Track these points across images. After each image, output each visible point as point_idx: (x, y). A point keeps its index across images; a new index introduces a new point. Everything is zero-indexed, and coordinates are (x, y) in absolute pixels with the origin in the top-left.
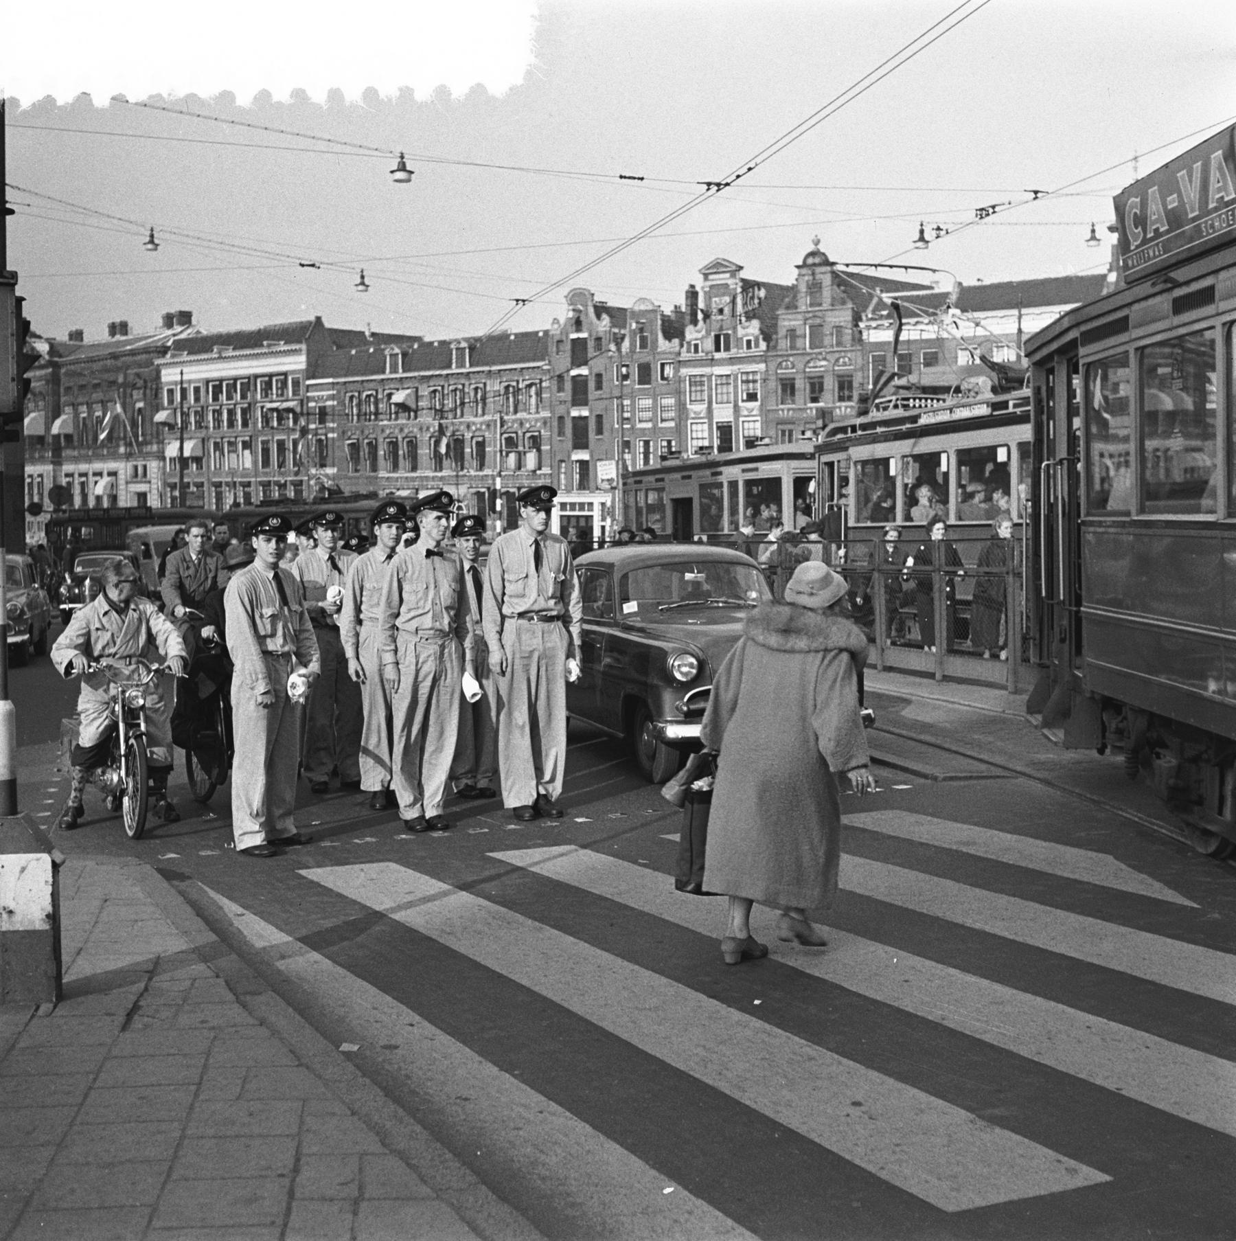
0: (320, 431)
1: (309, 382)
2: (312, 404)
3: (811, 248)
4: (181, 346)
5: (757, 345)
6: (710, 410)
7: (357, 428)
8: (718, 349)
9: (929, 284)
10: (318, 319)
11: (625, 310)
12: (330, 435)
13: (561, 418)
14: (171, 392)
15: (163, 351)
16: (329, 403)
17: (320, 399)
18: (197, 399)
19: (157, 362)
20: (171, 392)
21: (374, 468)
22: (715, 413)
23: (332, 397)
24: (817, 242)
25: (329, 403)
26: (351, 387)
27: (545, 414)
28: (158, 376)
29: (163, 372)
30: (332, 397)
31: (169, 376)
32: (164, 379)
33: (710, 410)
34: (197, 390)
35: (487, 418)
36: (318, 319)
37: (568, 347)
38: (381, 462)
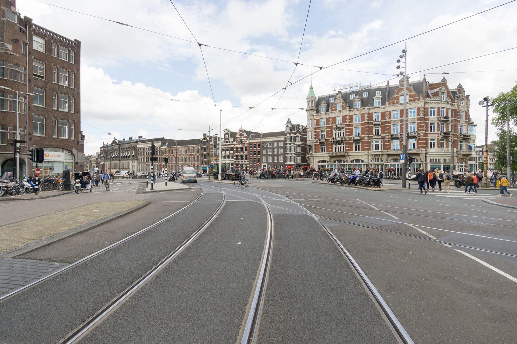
3: (240, 127)
4: (140, 141)
5: (232, 142)
6: (225, 153)
8: (226, 143)
9: (260, 133)
10: (163, 137)
11: (212, 136)
13: (202, 154)
14: (139, 149)
15: (137, 142)
20: (139, 149)
22: (226, 153)
24: (241, 126)
27: (200, 153)
33: (225, 153)
35: (190, 153)
36: (163, 137)
37: (203, 142)
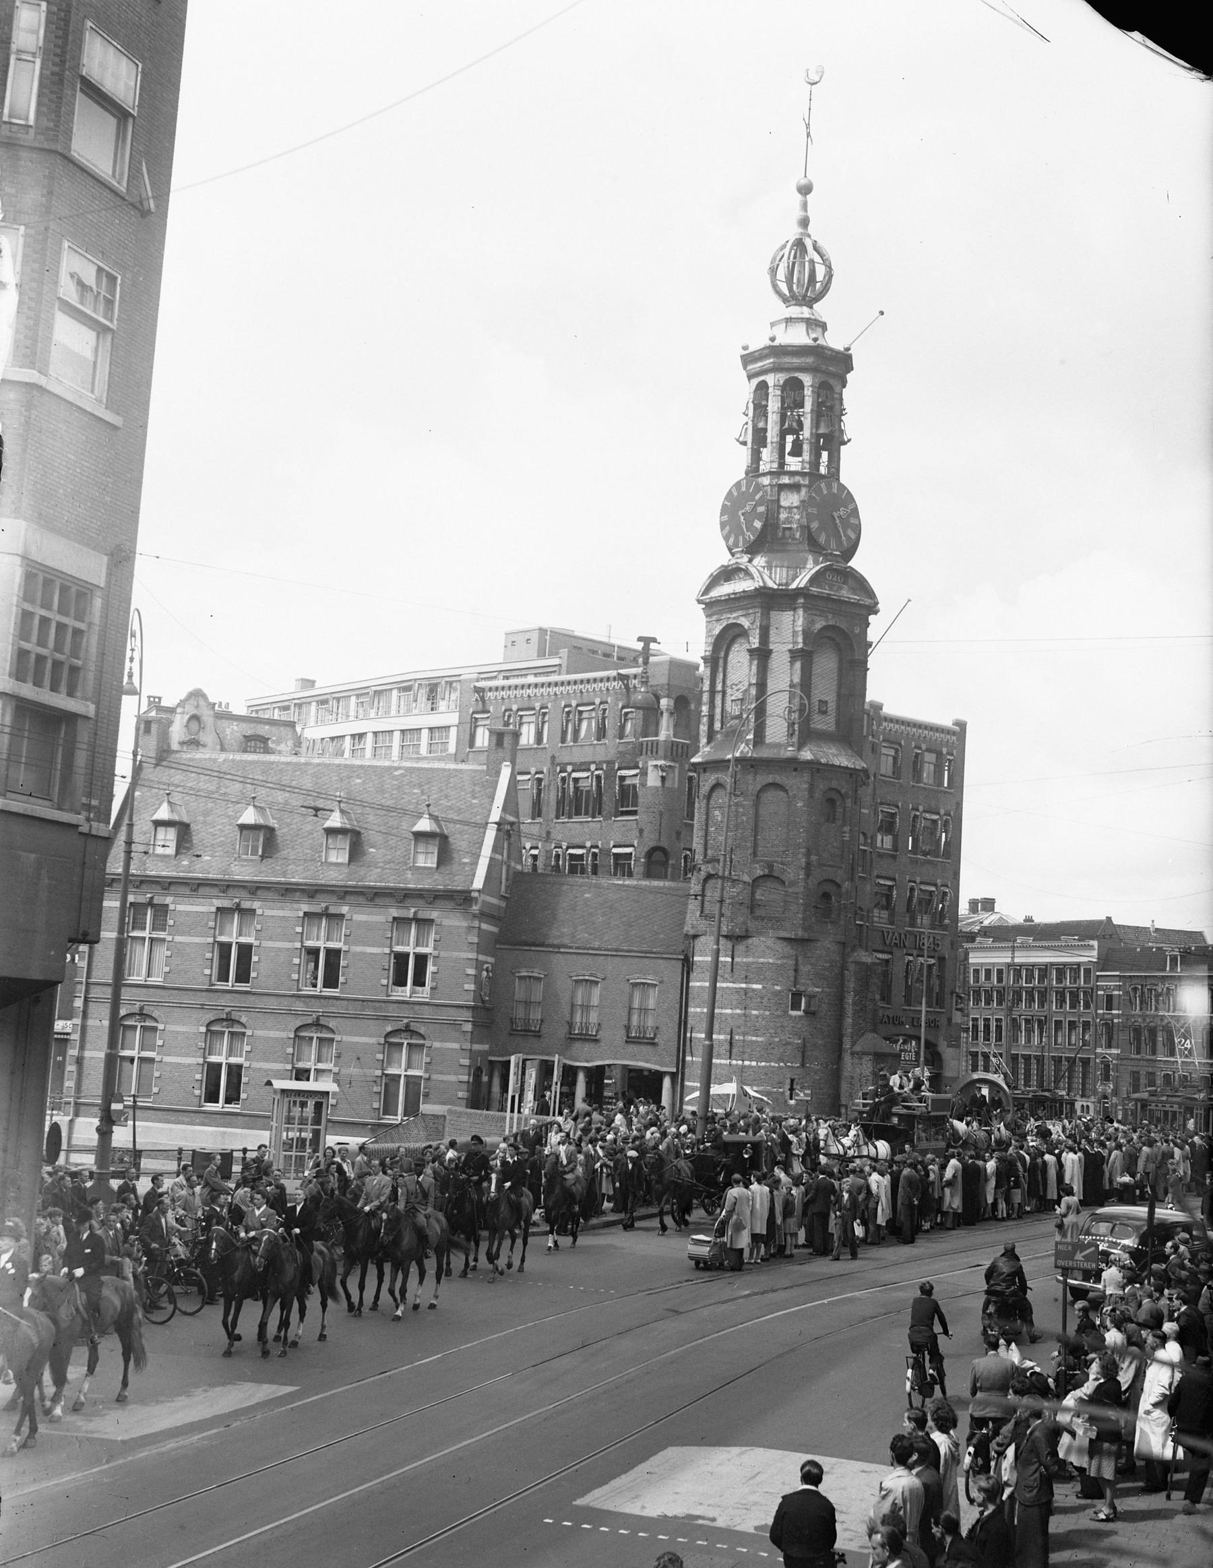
0: (1106, 1016)
1: (1098, 973)
2: (1100, 993)
4: (986, 932)
7: (1140, 1016)
12: (1116, 1021)
14: (976, 971)
16: (1116, 993)
17: (1108, 988)
18: (1000, 980)
19: (966, 945)
20: (976, 971)
21: (1154, 1053)
23: (1119, 988)
25: (1116, 993)
26: (1135, 981)
28: (966, 958)
29: (971, 955)
30: (1119, 988)
31: (975, 959)
32: (971, 961)
34: (1000, 972)
36: (1109, 919)
38: (1160, 1046)
